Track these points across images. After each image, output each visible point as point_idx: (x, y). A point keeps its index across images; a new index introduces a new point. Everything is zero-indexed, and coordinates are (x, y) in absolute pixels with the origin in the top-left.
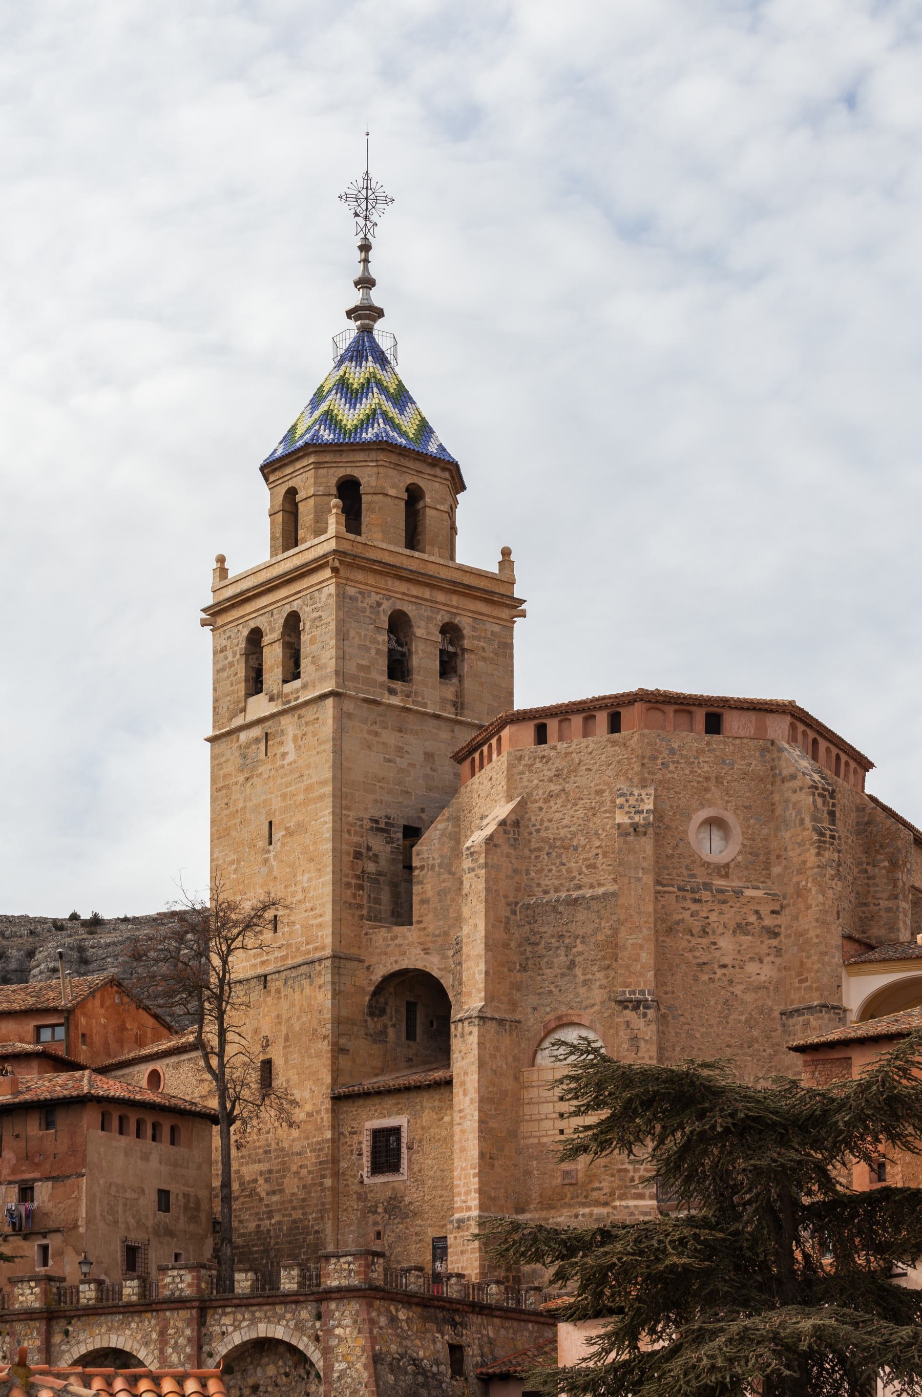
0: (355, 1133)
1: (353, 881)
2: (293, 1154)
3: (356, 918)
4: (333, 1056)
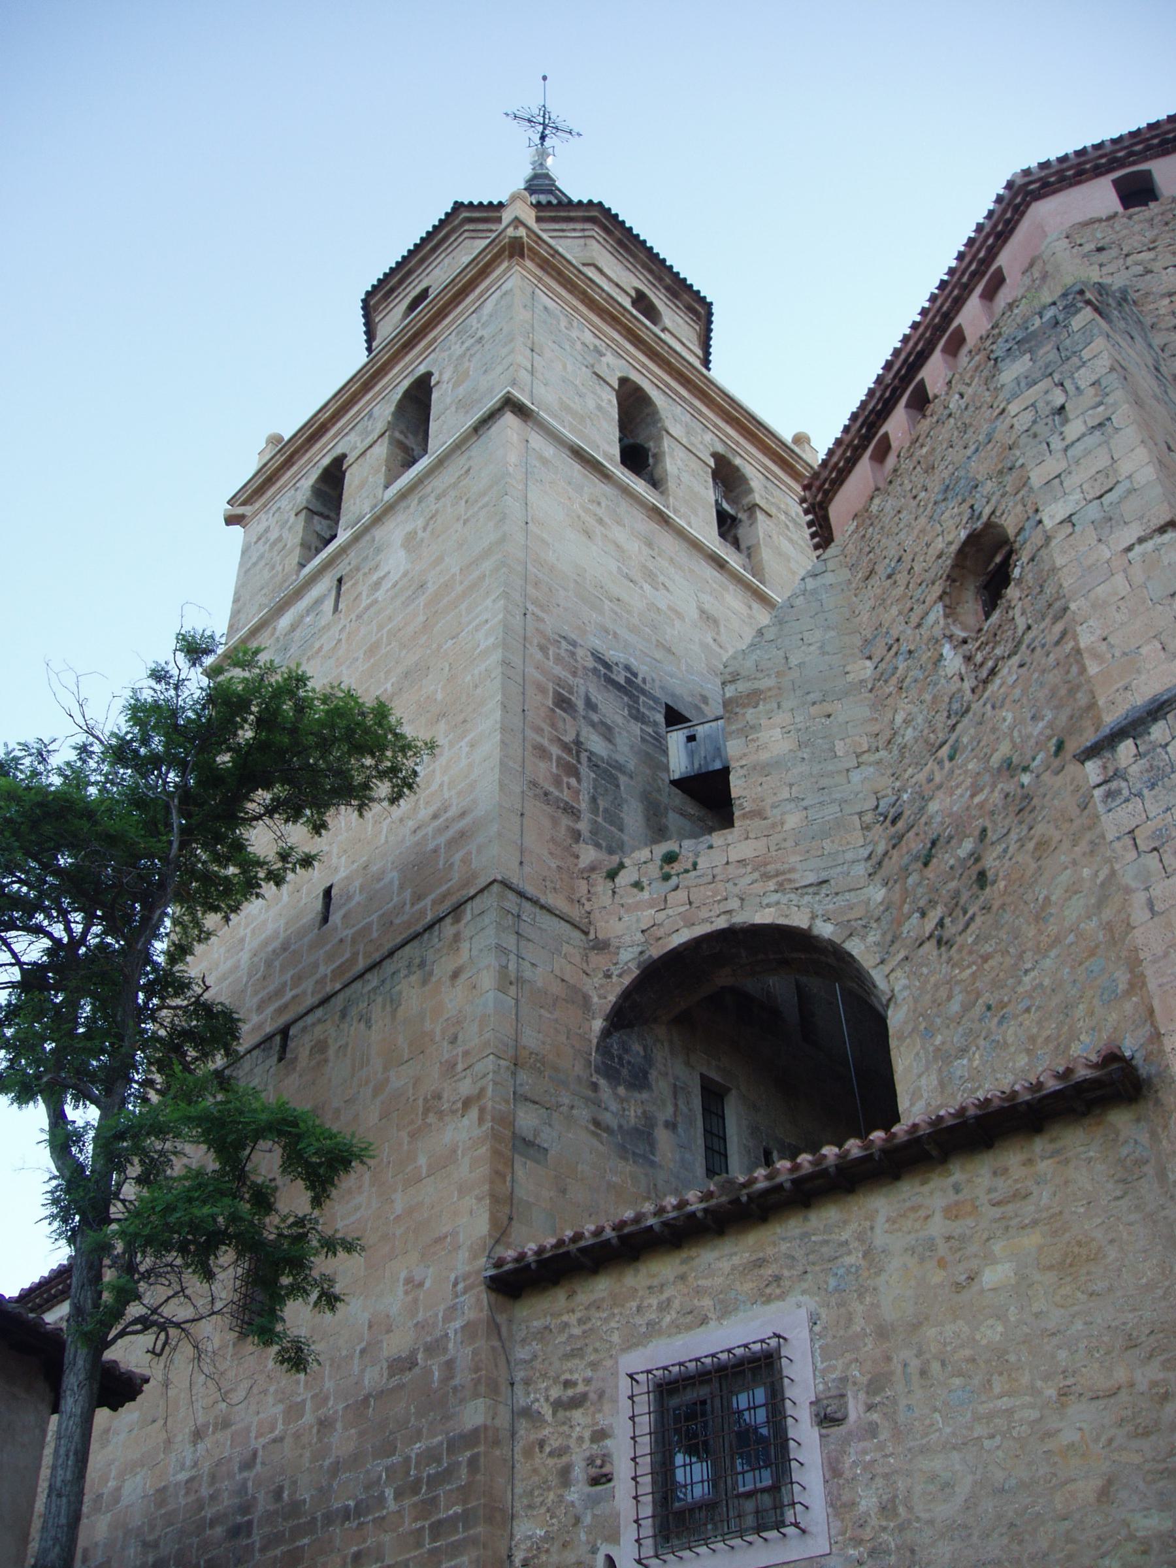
0: (577, 1402)
1: (555, 750)
2: (329, 1519)
3: (563, 830)
4: (496, 1153)
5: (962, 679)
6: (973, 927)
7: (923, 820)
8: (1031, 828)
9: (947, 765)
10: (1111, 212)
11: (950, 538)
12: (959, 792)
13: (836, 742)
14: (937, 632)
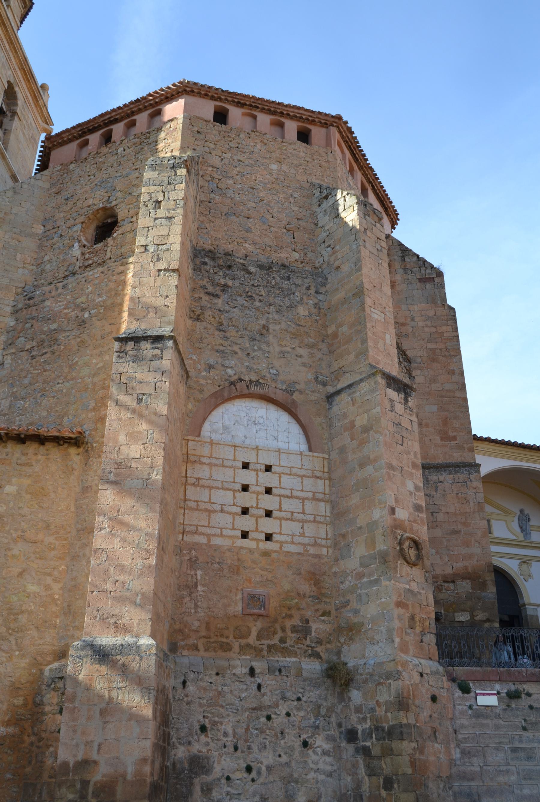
5: (77, 260)
6: (45, 356)
7: (41, 306)
8: (81, 334)
9: (60, 290)
10: (208, 120)
11: (96, 202)
12: (60, 304)
13: (18, 254)
14: (75, 235)
